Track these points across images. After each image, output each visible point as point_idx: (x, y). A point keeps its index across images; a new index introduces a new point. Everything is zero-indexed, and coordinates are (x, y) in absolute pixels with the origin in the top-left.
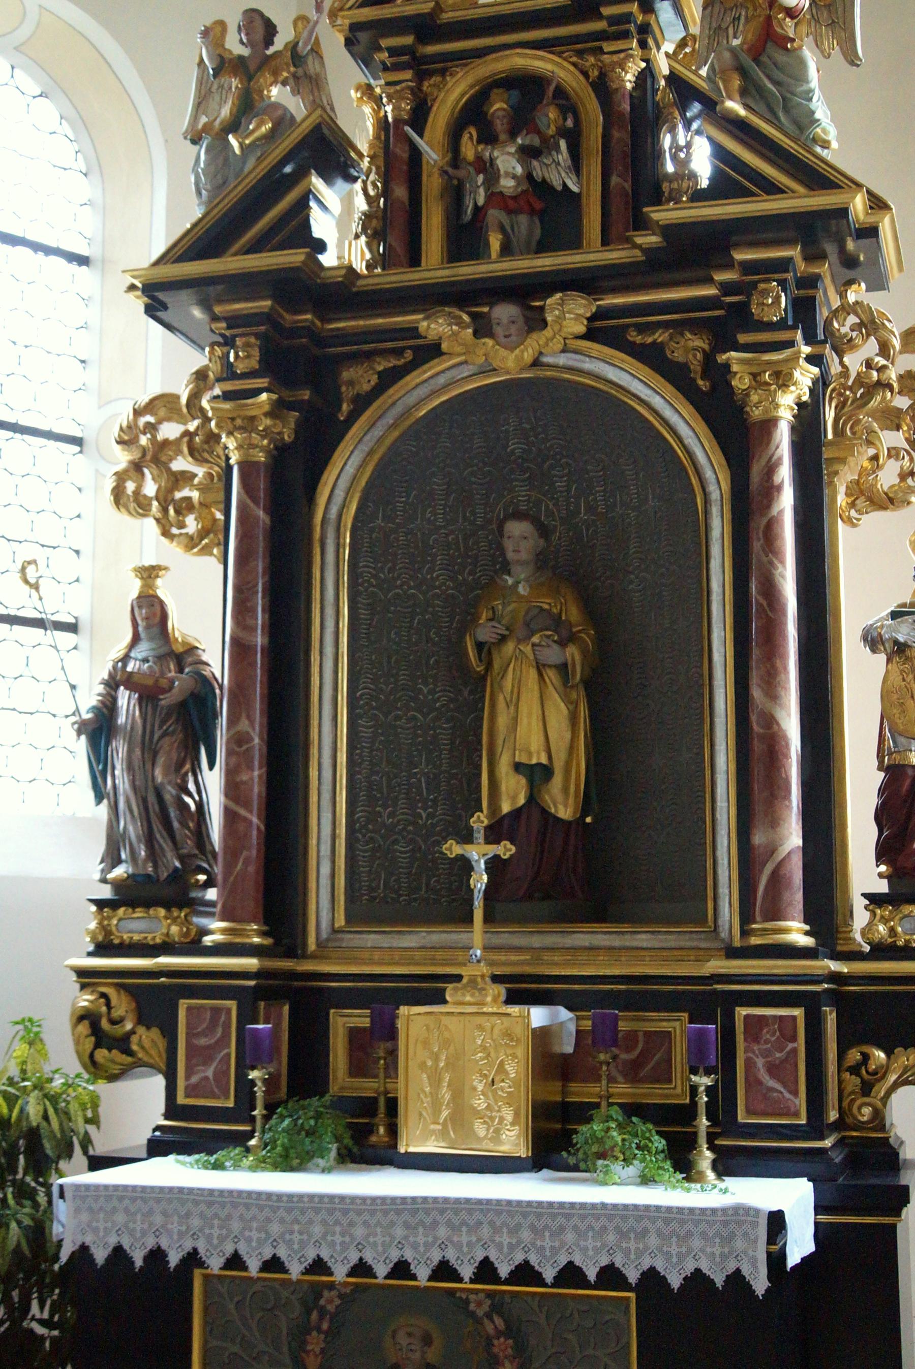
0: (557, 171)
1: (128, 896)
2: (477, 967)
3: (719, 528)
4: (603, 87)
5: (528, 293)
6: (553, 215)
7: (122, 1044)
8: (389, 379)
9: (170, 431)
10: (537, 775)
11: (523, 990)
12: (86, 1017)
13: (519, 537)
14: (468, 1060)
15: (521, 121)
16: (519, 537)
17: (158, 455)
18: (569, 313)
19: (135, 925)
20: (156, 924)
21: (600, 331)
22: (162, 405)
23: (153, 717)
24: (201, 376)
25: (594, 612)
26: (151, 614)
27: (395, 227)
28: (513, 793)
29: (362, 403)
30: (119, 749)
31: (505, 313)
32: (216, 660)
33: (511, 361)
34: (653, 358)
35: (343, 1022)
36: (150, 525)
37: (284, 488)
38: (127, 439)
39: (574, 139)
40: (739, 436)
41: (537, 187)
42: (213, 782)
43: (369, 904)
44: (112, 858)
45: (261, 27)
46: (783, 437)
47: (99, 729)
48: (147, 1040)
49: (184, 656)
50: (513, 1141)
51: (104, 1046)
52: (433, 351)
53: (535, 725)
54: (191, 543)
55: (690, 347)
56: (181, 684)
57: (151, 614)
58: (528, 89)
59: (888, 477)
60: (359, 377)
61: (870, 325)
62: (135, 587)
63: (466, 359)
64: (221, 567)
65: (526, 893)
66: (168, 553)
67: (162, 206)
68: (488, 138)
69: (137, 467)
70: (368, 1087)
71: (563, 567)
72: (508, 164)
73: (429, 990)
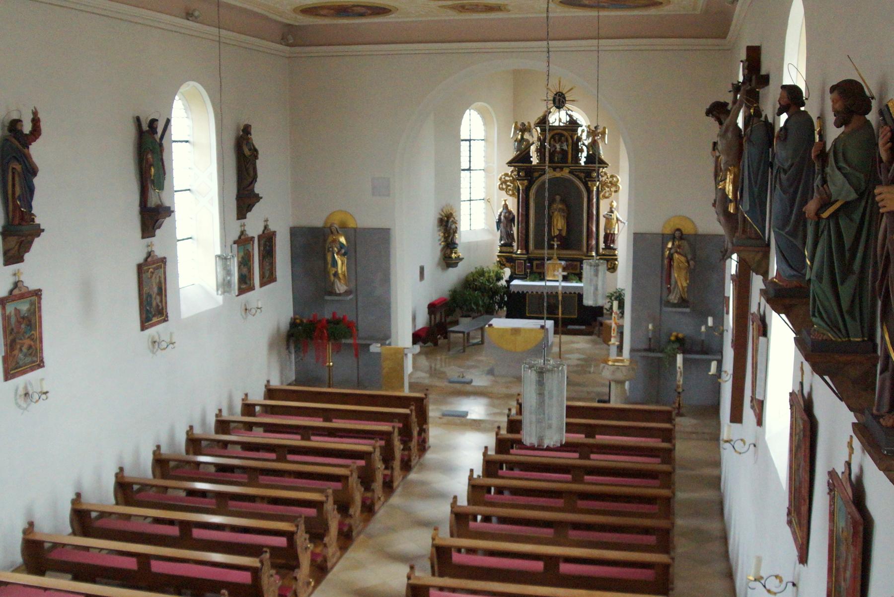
0: (565, 147)
1: (501, 246)
2: (555, 256)
3: (585, 200)
4: (572, 137)
5: (562, 169)
6: (564, 153)
7: (504, 265)
9: (507, 178)
10: (560, 230)
11: (560, 259)
12: (499, 262)
15: (560, 140)
16: (558, 198)
17: (505, 182)
18: (567, 170)
19: (505, 249)
20: (509, 249)
21: (571, 172)
22: (506, 175)
23: (506, 221)
24: (512, 172)
25: (567, 206)
27: (541, 151)
28: (557, 233)
30: (502, 225)
31: (558, 170)
32: (515, 213)
33: (558, 174)
34: (577, 176)
35: (535, 263)
36: (504, 192)
37: (527, 190)
38: (500, 179)
39: (567, 141)
40: (589, 192)
41: (562, 150)
42: (515, 229)
44: (501, 240)
45: (523, 124)
46: (594, 193)
47: (499, 222)
48: (508, 264)
49: (510, 212)
51: (502, 265)
53: (559, 224)
55: (582, 175)
56: (511, 216)
58: (561, 135)
59: (607, 194)
60: (536, 174)
61: (606, 174)
64: (516, 200)
67: (512, 154)
68: (555, 140)
70: (539, 271)
71: (563, 201)
72: (558, 147)
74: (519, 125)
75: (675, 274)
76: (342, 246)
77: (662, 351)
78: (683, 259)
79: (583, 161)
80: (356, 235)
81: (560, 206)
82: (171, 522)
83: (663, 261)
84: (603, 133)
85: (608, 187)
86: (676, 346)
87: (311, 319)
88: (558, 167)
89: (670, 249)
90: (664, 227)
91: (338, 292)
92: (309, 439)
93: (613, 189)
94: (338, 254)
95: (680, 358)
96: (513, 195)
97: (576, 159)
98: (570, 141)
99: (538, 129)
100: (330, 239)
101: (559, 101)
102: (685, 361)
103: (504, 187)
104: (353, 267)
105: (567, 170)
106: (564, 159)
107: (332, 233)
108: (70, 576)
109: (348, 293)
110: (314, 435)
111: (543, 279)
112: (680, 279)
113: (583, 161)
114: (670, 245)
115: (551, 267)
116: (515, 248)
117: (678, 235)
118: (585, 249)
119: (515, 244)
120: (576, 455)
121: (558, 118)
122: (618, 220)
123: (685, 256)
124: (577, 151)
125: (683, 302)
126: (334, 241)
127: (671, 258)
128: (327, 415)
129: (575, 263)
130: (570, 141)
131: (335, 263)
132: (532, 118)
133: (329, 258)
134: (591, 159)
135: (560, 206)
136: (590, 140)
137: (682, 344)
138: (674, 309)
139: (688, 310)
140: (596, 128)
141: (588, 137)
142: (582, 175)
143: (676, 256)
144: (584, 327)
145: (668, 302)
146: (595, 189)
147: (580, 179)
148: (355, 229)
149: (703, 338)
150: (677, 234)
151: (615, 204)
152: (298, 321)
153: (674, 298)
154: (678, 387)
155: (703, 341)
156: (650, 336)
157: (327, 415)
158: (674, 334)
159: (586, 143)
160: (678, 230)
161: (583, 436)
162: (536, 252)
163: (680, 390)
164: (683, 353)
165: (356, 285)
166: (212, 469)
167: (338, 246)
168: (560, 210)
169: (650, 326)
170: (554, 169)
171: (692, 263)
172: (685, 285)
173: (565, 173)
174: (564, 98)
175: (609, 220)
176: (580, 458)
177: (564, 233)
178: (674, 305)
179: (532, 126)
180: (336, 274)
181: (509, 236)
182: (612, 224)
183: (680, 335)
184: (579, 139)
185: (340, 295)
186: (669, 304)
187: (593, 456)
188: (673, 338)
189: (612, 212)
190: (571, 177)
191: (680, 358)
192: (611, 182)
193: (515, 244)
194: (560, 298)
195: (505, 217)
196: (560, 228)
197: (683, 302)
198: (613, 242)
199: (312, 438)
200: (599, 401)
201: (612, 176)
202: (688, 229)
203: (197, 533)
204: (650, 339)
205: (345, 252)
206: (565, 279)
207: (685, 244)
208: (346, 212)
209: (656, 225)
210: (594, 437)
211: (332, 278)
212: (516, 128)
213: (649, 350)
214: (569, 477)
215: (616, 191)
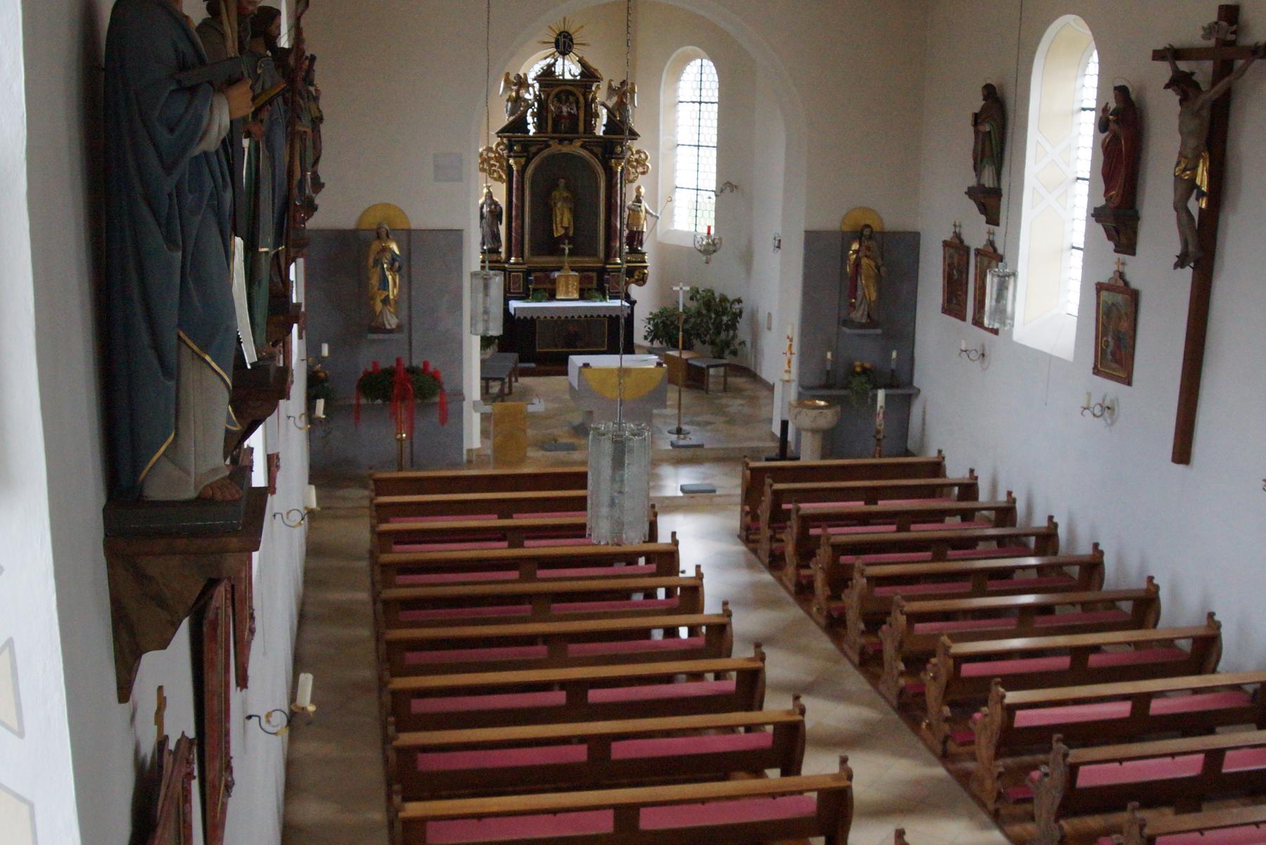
5: (571, 141)
6: (573, 118)
8: (540, 150)
10: (566, 229)
13: (562, 181)
14: (567, 282)
16: (562, 181)
18: (578, 143)
20: (495, 257)
21: (582, 146)
24: (498, 145)
26: (490, 195)
29: (536, 154)
33: (565, 149)
34: (591, 152)
37: (522, 172)
39: (577, 102)
40: (610, 174)
41: (570, 113)
42: (502, 229)
43: (536, 250)
44: (483, 244)
49: (496, 204)
50: (576, 296)
52: (549, 146)
54: (495, 179)
57: (490, 195)
60: (533, 149)
61: (630, 149)
62: (485, 191)
63: (555, 148)
65: (572, 253)
66: (491, 182)
68: (560, 101)
69: (482, 163)
71: (567, 188)
72: (565, 109)
73: (559, 269)
74: (512, 78)
75: (862, 281)
76: (394, 258)
77: (846, 388)
78: (873, 264)
79: (600, 131)
80: (409, 237)
81: (565, 194)
82: (546, 686)
83: (843, 267)
84: (633, 92)
85: (633, 167)
86: (864, 379)
87: (370, 369)
88: (566, 139)
89: (856, 252)
90: (843, 222)
91: (388, 327)
92: (521, 546)
93: (640, 169)
94: (391, 269)
95: (881, 394)
96: (500, 179)
97: (590, 128)
98: (581, 99)
99: (537, 85)
100: (376, 246)
101: (564, 44)
102: (888, 398)
103: (486, 166)
104: (405, 290)
105: (578, 143)
106: (574, 129)
107: (379, 237)
108: (1254, 726)
109: (399, 328)
110: (528, 538)
111: (552, 297)
112: (868, 289)
113: (600, 131)
114: (855, 246)
115: (562, 280)
116: (503, 256)
117: (862, 233)
118: (602, 255)
119: (503, 250)
120: (894, 527)
121: (568, 69)
122: (647, 212)
123: (874, 259)
124: (592, 115)
125: (872, 323)
126: (385, 249)
127: (857, 265)
128: (505, 508)
129: (590, 274)
130: (581, 99)
131: (384, 284)
132: (533, 70)
133: (375, 281)
134: (610, 126)
135: (565, 194)
136: (615, 99)
137: (874, 377)
138: (860, 331)
139: (879, 331)
140: (623, 83)
141: (609, 97)
142: (598, 150)
143: (865, 261)
144: (533, 365)
145: (852, 321)
146: (619, 169)
147: (596, 155)
148: (409, 231)
149: (893, 366)
150: (867, 232)
151: (643, 190)
152: (322, 375)
153: (859, 315)
154: (878, 432)
155: (893, 371)
156: (829, 368)
157: (505, 508)
158: (858, 363)
159: (610, 104)
160: (868, 226)
161: (862, 503)
162: (536, 259)
163: (881, 436)
164: (885, 387)
165: (410, 317)
166: (1033, 575)
167: (388, 256)
168: (565, 199)
169: (829, 355)
170: (561, 141)
171: (883, 269)
172: (874, 296)
173: (576, 148)
174: (571, 40)
175: (635, 212)
176: (899, 530)
177: (571, 233)
178: (862, 326)
179: (530, 81)
180: (386, 301)
181: (495, 237)
182: (639, 218)
183: (867, 365)
184: (594, 99)
185: (391, 331)
186: (847, 322)
187: (913, 527)
188: (858, 369)
189: (639, 201)
190: (583, 153)
191: (881, 394)
192: (637, 160)
193: (503, 250)
194: (622, 321)
195: (491, 212)
196: (566, 224)
197: (872, 323)
198: (641, 244)
199: (527, 543)
200: (767, 460)
201: (638, 152)
202: (876, 228)
203: (595, 696)
204: (828, 372)
205: (402, 266)
206: (582, 297)
207: (872, 244)
208: (388, 205)
209: (831, 221)
210: (876, 503)
211: (379, 306)
212: (507, 81)
213: (827, 386)
214: (928, 554)
215: (643, 173)
